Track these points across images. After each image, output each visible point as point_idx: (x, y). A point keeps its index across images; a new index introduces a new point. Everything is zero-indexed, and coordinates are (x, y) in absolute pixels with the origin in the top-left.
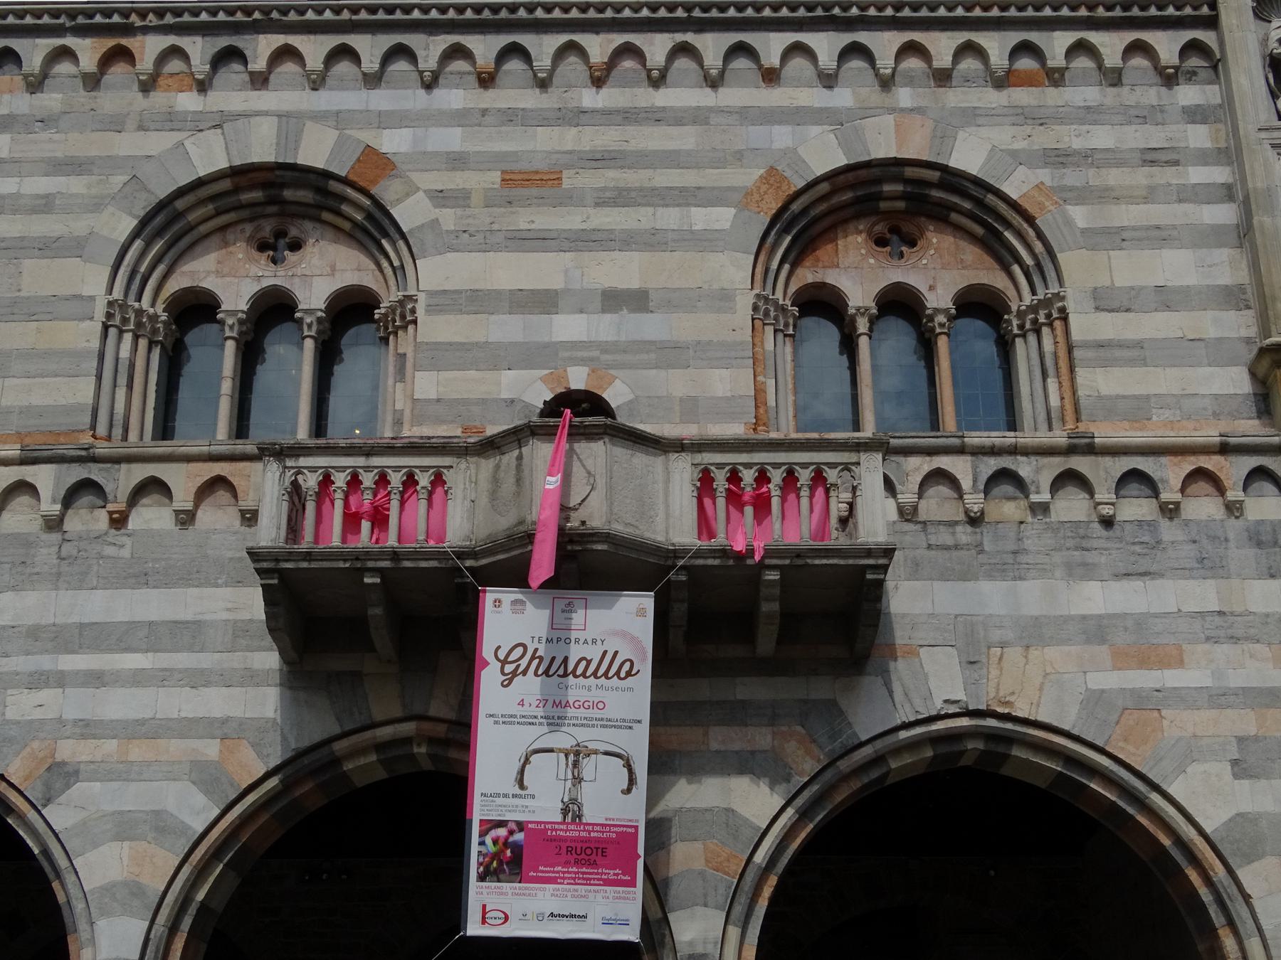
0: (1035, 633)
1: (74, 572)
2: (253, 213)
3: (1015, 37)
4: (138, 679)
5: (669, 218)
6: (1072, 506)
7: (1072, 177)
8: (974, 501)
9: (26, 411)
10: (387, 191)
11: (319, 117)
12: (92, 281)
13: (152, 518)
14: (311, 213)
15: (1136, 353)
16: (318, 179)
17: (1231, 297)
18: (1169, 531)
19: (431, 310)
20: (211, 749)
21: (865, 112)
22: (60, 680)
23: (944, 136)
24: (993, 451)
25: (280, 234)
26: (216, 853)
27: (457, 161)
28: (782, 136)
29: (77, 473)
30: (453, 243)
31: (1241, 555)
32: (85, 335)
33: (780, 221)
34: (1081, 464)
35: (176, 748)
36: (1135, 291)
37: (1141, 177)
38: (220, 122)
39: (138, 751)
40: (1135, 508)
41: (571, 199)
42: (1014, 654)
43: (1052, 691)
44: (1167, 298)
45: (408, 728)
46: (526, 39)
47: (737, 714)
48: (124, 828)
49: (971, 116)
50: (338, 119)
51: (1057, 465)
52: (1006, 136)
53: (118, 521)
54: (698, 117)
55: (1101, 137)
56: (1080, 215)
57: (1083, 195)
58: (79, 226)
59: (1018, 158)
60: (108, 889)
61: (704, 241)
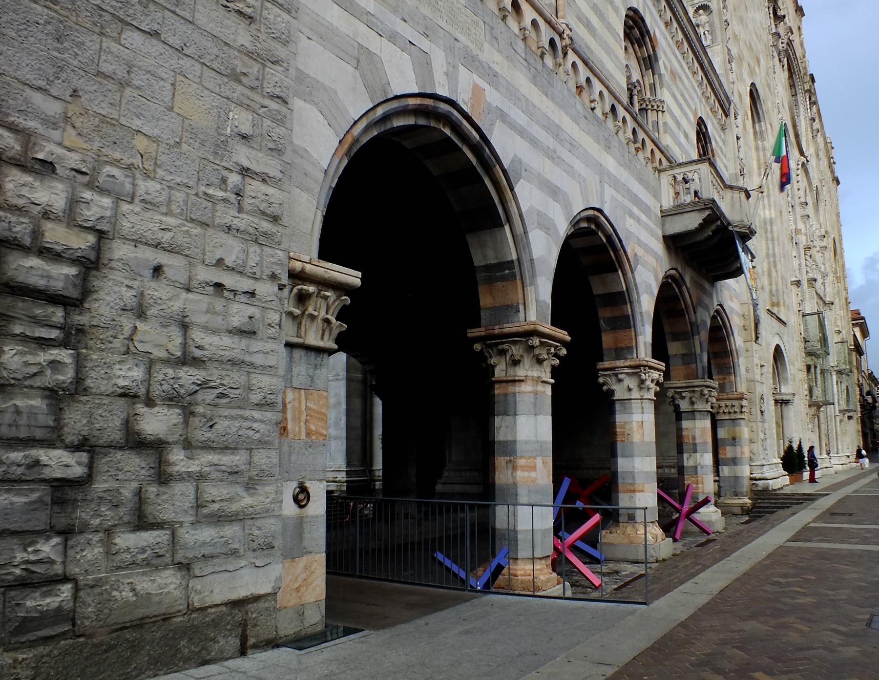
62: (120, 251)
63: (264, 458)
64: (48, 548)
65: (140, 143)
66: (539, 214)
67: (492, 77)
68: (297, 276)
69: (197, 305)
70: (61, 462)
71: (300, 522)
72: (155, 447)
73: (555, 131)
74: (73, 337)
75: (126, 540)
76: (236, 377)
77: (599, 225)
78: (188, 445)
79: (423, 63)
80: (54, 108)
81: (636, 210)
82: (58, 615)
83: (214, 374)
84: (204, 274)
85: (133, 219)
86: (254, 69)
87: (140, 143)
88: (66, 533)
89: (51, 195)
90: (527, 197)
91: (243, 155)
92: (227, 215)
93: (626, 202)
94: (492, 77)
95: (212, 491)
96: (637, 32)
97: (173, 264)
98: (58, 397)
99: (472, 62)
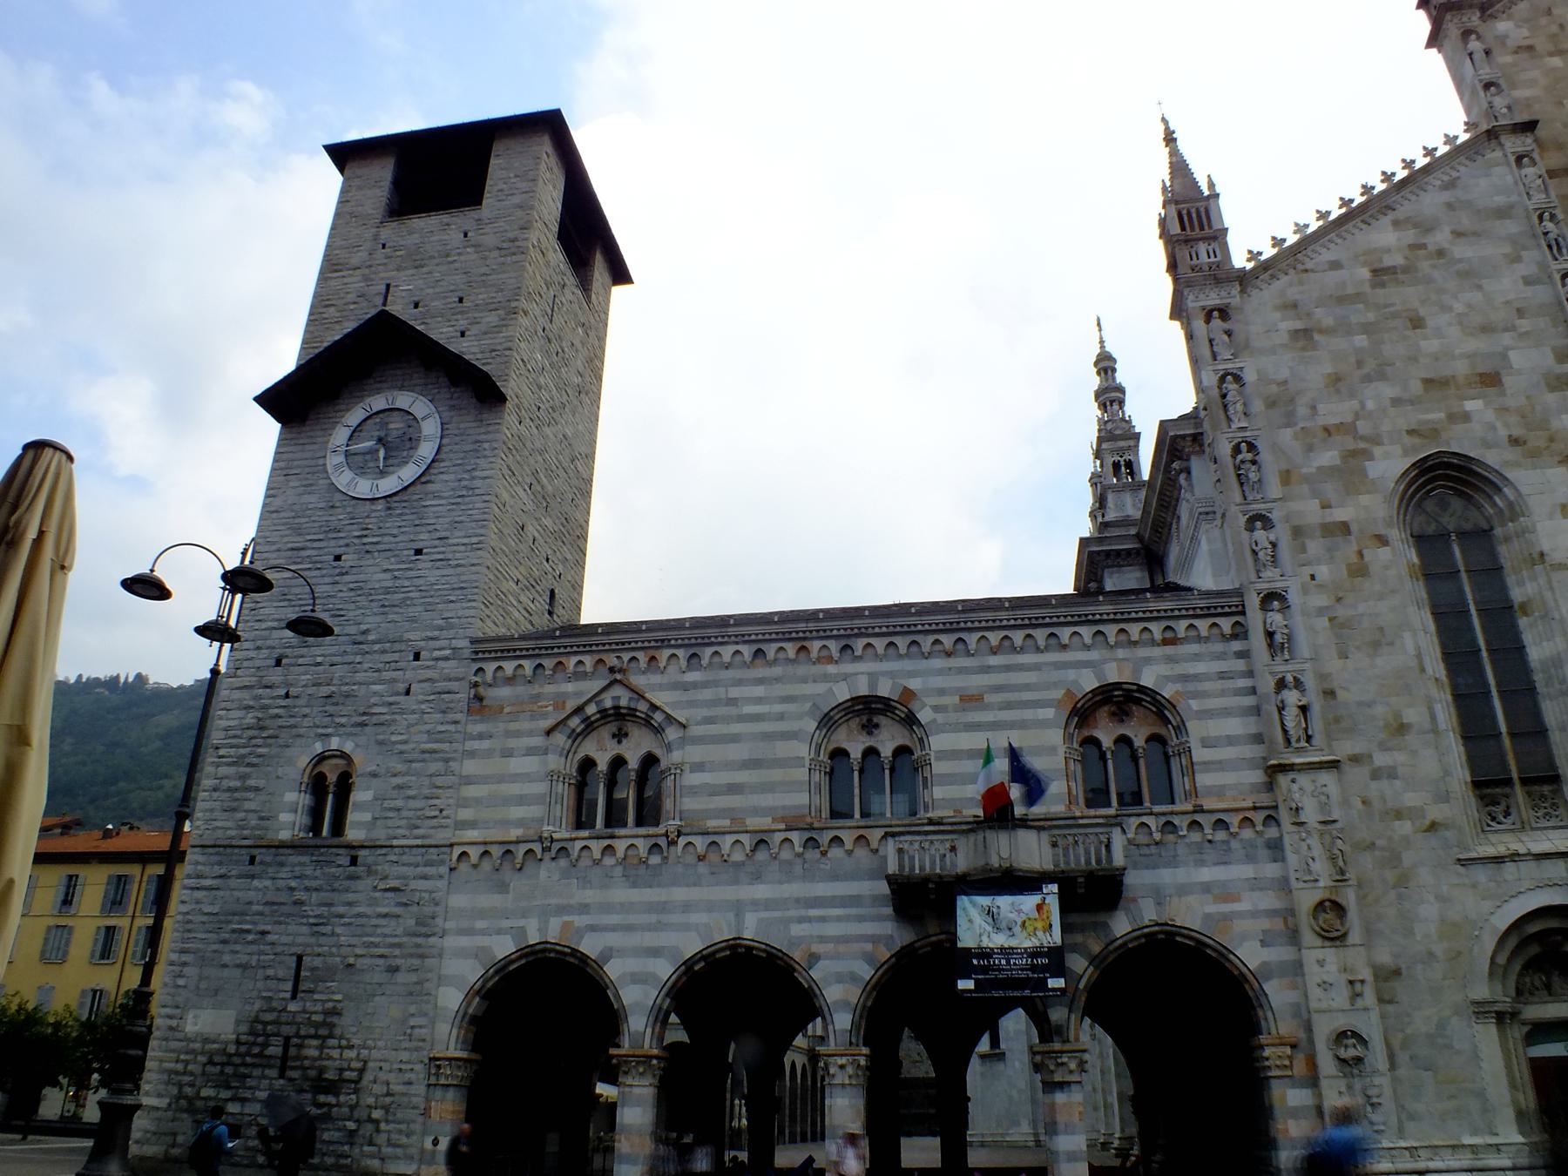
0: (1183, 890)
1: (809, 876)
2: (859, 713)
3: (1164, 624)
4: (839, 919)
5: (1028, 714)
6: (1195, 837)
7: (1191, 687)
8: (1157, 836)
9: (784, 807)
10: (914, 706)
11: (885, 674)
12: (803, 750)
13: (836, 852)
14: (883, 712)
15: (1220, 766)
16: (886, 701)
17: (1258, 739)
18: (1235, 844)
19: (938, 759)
20: (869, 947)
21: (1104, 661)
22: (810, 920)
23: (1137, 671)
24: (1164, 814)
25: (869, 720)
26: (874, 988)
27: (942, 692)
28: (1071, 674)
29: (807, 835)
30: (943, 729)
31: (1263, 853)
32: (801, 774)
33: (1074, 712)
34: (1198, 817)
35: (856, 947)
36: (1218, 738)
37: (1220, 685)
38: (845, 677)
39: (842, 948)
40: (1221, 835)
42: (1175, 899)
43: (1190, 914)
44: (1231, 741)
45: (942, 937)
46: (963, 635)
48: (839, 978)
49: (1148, 661)
50: (891, 674)
51: (1189, 818)
52: (1164, 670)
53: (824, 854)
54: (1036, 667)
55: (1201, 668)
56: (1195, 704)
58: (794, 726)
59: (1168, 679)
60: (836, 1002)
61: (1042, 724)
62: (371, 1064)
64: (346, 1148)
66: (633, 974)
67: (584, 908)
69: (392, 1077)
70: (351, 1125)
71: (434, 1153)
72: (377, 1122)
73: (662, 907)
74: (356, 1091)
75: (366, 1148)
76: (405, 1099)
78: (387, 1122)
79: (522, 931)
80: (354, 1029)
82: (346, 1166)
83: (396, 1099)
85: (375, 1054)
88: (352, 1144)
89: (352, 1054)
90: (613, 970)
92: (404, 1045)
94: (584, 908)
95: (394, 1137)
98: (352, 1108)
99: (562, 910)
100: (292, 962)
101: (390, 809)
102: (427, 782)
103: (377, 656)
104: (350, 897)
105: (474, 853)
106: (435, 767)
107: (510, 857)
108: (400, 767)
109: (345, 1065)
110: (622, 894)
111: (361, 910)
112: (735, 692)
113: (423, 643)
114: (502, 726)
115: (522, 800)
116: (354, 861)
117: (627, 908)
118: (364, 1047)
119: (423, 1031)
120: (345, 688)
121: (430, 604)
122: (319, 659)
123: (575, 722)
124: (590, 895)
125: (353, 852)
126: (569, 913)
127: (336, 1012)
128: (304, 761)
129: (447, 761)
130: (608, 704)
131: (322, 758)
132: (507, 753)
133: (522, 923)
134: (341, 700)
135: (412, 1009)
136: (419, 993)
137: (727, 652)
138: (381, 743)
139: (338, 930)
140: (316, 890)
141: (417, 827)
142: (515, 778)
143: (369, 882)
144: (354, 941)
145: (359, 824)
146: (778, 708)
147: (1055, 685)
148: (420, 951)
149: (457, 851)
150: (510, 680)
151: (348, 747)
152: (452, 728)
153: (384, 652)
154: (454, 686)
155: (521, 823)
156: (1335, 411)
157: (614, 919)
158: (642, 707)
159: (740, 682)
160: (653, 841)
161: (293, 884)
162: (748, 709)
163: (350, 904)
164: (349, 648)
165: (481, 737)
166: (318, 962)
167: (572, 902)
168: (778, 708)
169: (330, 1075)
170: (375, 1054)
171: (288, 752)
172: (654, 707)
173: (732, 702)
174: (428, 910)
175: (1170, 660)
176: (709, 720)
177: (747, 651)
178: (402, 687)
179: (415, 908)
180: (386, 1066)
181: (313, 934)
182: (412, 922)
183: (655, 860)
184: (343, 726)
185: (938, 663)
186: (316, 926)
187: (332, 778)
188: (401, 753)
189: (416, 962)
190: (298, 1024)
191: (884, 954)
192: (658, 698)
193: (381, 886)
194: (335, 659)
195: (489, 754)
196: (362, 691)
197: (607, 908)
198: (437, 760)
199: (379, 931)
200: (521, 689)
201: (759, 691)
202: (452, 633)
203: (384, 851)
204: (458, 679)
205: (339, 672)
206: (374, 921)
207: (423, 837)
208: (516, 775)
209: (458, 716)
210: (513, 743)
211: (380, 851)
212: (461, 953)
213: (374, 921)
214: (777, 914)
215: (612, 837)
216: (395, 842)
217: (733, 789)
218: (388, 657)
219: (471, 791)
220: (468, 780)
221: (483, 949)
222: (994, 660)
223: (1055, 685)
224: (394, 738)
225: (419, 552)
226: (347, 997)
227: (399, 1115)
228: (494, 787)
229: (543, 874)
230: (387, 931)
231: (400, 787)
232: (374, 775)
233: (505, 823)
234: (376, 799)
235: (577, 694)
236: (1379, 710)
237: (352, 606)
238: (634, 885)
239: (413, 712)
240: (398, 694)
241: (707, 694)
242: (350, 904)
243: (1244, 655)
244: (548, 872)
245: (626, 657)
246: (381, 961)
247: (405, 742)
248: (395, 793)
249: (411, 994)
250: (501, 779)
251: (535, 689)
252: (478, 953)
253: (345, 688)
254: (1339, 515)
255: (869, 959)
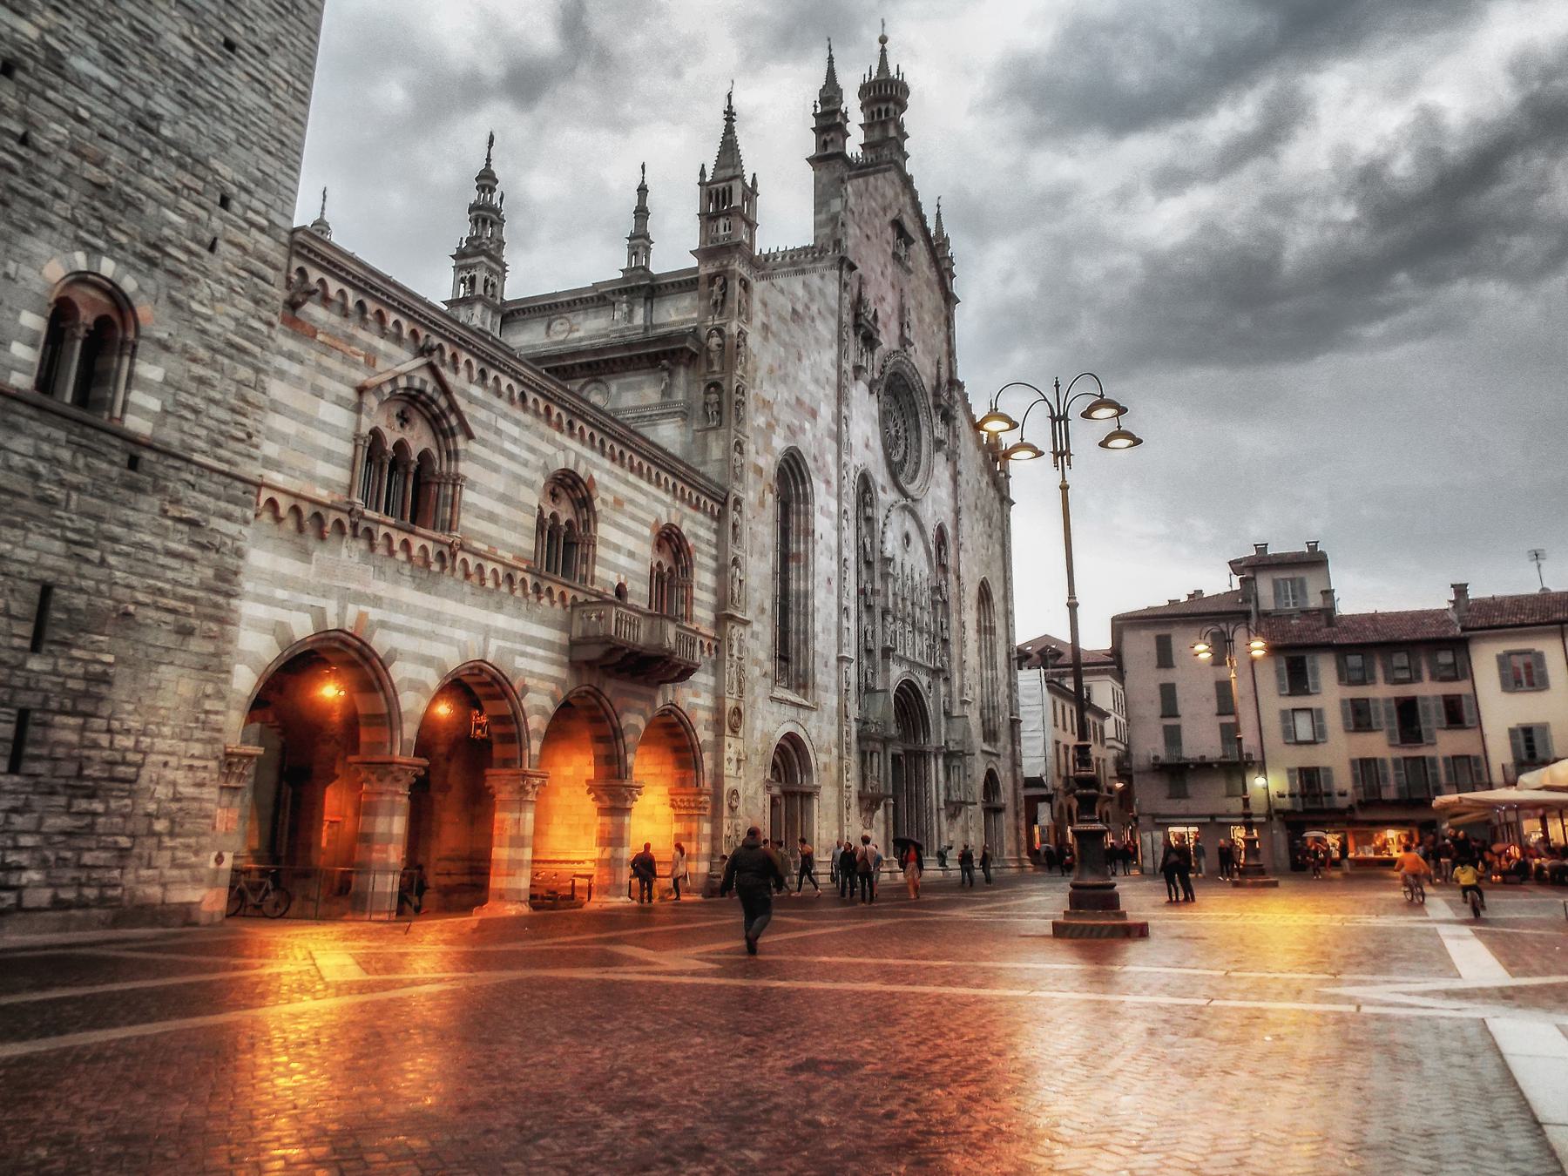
1: (528, 616)
13: (545, 601)
20: (553, 686)
27: (607, 489)
41: (623, 513)
47: (640, 697)
50: (588, 461)
54: (645, 493)
55: (703, 532)
57: (701, 552)
62: (153, 758)
63: (205, 841)
65: (162, 712)
66: (410, 680)
67: (376, 601)
68: (227, 755)
77: (481, 670)
79: (320, 615)
81: (530, 649)
84: (186, 762)
86: (215, 661)
87: (162, 712)
90: (399, 672)
91: (208, 705)
92: (198, 734)
93: (518, 646)
94: (376, 601)
96: (569, 481)
97: (173, 761)
99: (359, 598)
100: (34, 591)
101: (187, 407)
102: (233, 389)
103: (173, 168)
104: (132, 516)
105: (284, 503)
106: (244, 373)
107: (310, 523)
108: (202, 353)
109: (118, 757)
110: (408, 594)
111: (148, 538)
112: (503, 424)
113: (235, 190)
114: (312, 355)
115: (329, 456)
116: (133, 463)
117: (410, 610)
118: (145, 734)
119: (220, 718)
120: (128, 189)
121: (245, 137)
122: (84, 114)
123: (388, 389)
124: (381, 588)
125: (132, 447)
126: (367, 604)
127: (104, 679)
128: (55, 271)
129: (258, 370)
130: (417, 384)
131: (80, 278)
132: (318, 393)
133: (321, 603)
134: (121, 205)
135: (209, 689)
136: (215, 667)
137: (505, 381)
138: (175, 303)
139: (112, 560)
140: (77, 488)
141: (219, 445)
142: (324, 426)
143: (155, 501)
144: (134, 581)
145: (143, 411)
146: (526, 455)
147: (651, 512)
148: (223, 614)
149: (265, 495)
150: (326, 300)
151: (129, 284)
152: (264, 328)
153: (181, 166)
154: (270, 273)
155: (327, 483)
156: (768, 392)
157: (399, 619)
158: (443, 402)
159: (505, 416)
160: (439, 548)
161: (41, 468)
162: (508, 446)
163: (128, 525)
164: (132, 128)
165: (291, 356)
166: (80, 601)
167: (368, 591)
168: (526, 455)
169: (92, 771)
170: (161, 744)
171: (28, 243)
172: (453, 407)
173: (498, 432)
174: (230, 561)
175: (694, 521)
176: (484, 443)
177: (517, 389)
178: (207, 238)
179: (213, 555)
180: (173, 761)
181: (71, 556)
182: (210, 573)
183: (436, 567)
184: (121, 247)
185: (607, 463)
186: (77, 547)
187: (87, 317)
188: (204, 332)
189: (214, 627)
190: (15, 688)
191: (561, 696)
192: (462, 403)
193: (173, 511)
194: (109, 130)
195: (299, 382)
196: (150, 208)
197: (396, 606)
198: (246, 364)
199: (170, 574)
200: (335, 319)
201: (515, 431)
202: (269, 198)
203: (178, 464)
204: (275, 268)
205: (117, 157)
206: (162, 560)
207: (228, 462)
208: (325, 423)
209: (275, 319)
210: (323, 381)
211: (171, 462)
212: (257, 625)
213: (162, 560)
214: (508, 645)
215: (412, 532)
216: (197, 457)
217: (492, 518)
218: (187, 178)
219: (278, 422)
220: (276, 407)
221: (281, 624)
222: (632, 478)
223: (651, 512)
224: (195, 306)
225: (230, 45)
226: (120, 660)
227: (187, 826)
228: (303, 428)
229: (344, 552)
230: (181, 577)
231: (201, 381)
232: (165, 347)
233: (311, 477)
234: (166, 382)
235: (388, 357)
236: (757, 595)
237: (136, 61)
238: (419, 588)
239: (219, 281)
240: (200, 242)
241: (482, 414)
242: (128, 525)
243: (716, 532)
244: (349, 553)
245: (436, 340)
246: (169, 618)
247: (208, 319)
248: (193, 386)
249: (206, 668)
250: (310, 421)
251: (351, 328)
252: (279, 629)
253: (128, 189)
254: (761, 462)
255: (553, 696)
